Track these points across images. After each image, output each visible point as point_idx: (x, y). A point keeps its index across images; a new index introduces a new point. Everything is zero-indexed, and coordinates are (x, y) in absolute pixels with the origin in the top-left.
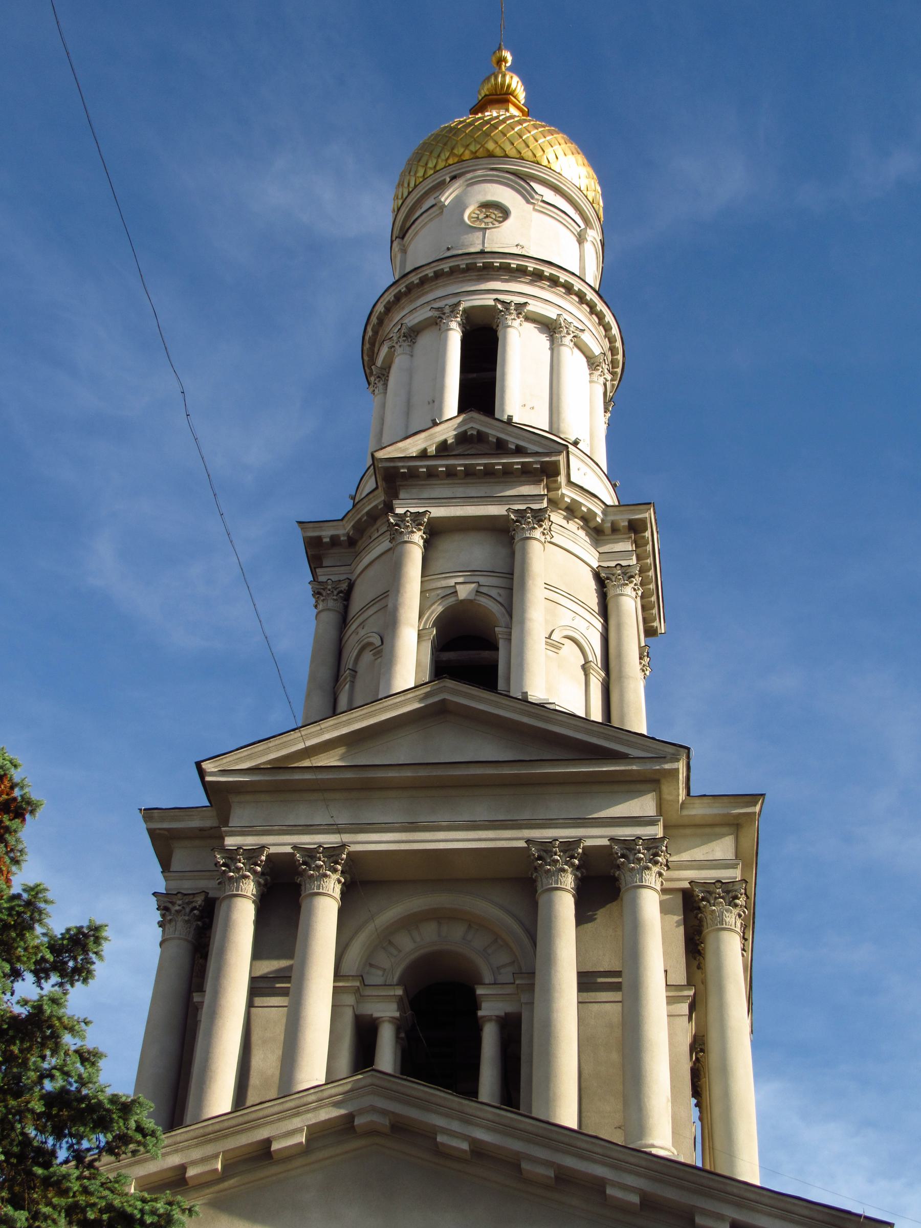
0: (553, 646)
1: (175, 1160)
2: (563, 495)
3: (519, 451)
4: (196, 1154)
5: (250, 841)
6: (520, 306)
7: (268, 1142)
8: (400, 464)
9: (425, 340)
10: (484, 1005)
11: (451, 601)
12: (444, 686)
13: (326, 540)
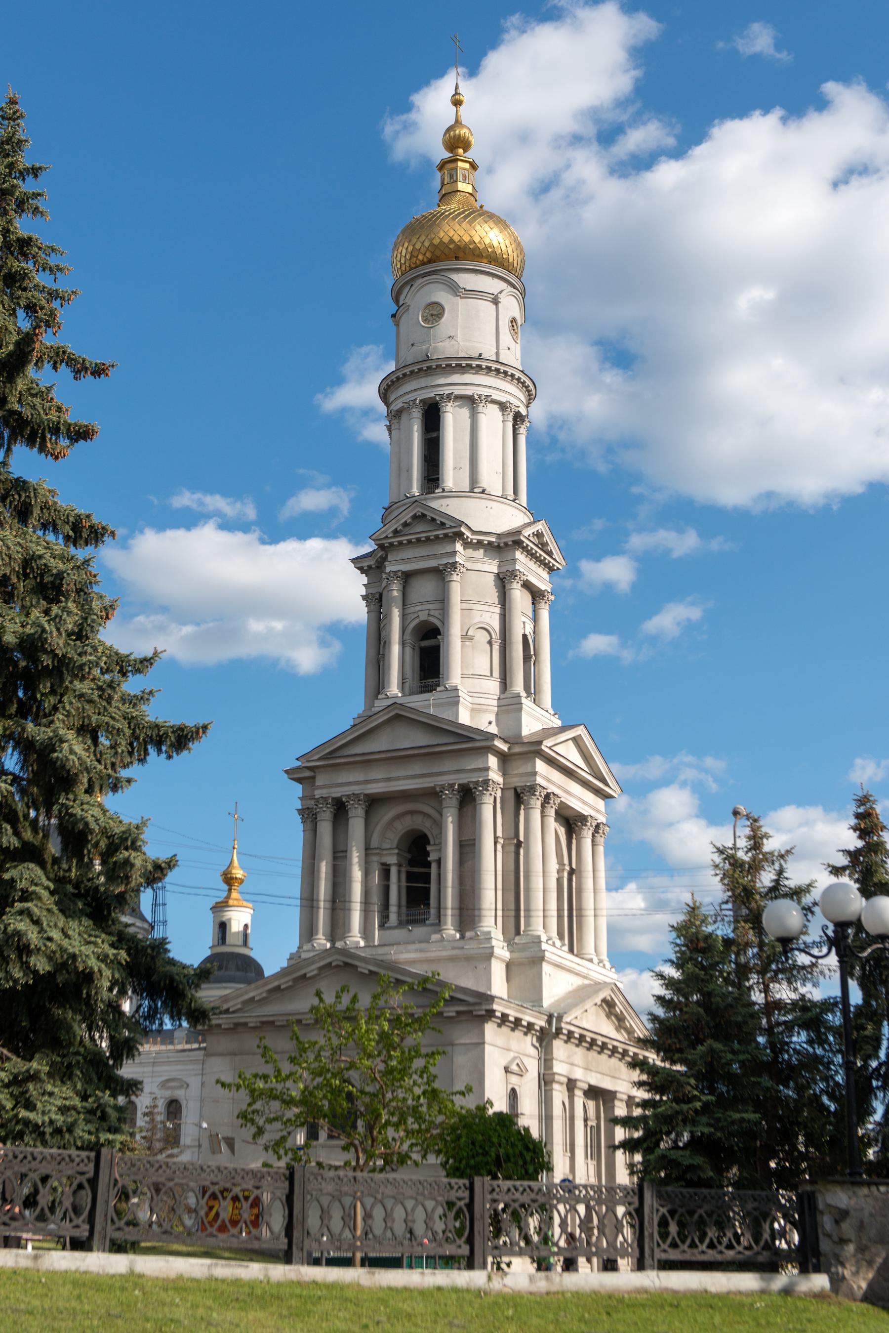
1: (276, 984)
3: (443, 524)
4: (283, 981)
5: (324, 792)
6: (449, 396)
7: (305, 975)
9: (404, 417)
10: (431, 855)
11: (416, 621)
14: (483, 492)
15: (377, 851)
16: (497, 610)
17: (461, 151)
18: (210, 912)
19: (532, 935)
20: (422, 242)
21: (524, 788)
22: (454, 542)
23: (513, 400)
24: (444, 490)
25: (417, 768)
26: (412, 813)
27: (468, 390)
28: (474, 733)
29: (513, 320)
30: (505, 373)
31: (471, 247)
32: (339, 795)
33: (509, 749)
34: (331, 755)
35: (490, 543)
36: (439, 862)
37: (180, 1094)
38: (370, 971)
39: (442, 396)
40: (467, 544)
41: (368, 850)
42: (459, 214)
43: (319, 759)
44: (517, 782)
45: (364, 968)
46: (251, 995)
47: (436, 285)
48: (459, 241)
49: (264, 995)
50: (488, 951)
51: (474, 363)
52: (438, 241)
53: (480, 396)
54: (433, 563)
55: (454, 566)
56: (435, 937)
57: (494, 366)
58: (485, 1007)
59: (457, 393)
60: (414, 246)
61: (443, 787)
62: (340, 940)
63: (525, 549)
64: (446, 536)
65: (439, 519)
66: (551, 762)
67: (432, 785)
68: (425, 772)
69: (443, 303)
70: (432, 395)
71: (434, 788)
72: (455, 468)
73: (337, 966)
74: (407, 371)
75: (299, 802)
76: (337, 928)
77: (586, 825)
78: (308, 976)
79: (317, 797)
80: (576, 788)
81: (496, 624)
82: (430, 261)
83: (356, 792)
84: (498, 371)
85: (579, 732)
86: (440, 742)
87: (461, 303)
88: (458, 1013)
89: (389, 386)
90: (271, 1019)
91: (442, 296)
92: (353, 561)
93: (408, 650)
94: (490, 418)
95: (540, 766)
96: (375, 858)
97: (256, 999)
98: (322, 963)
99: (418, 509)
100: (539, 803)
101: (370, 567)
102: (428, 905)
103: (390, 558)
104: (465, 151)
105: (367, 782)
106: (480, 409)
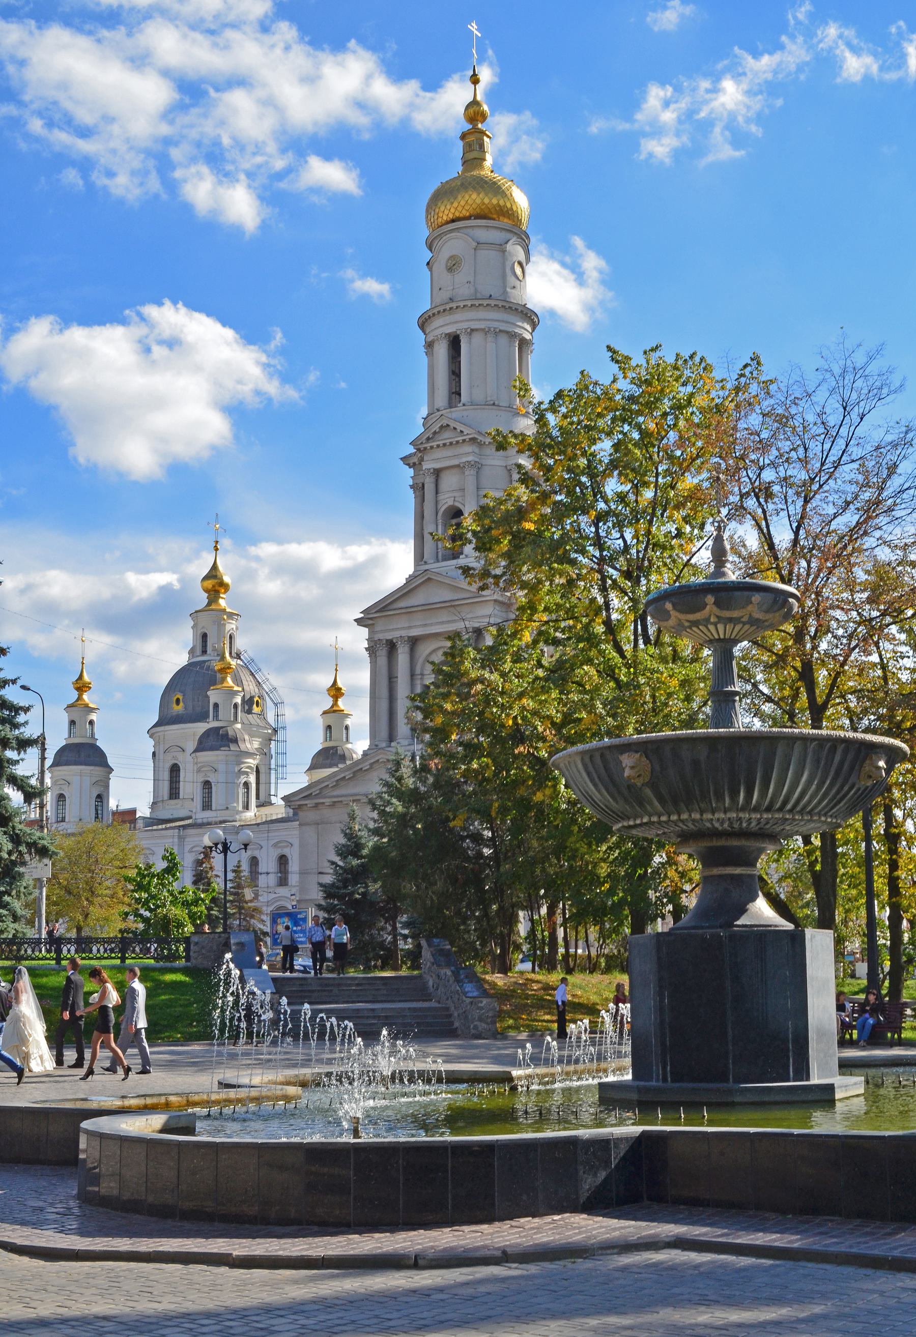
1: (343, 775)
3: (462, 432)
4: (347, 773)
25: (444, 616)
37: (286, 851)
41: (412, 675)
43: (376, 612)
54: (455, 462)
64: (464, 441)
68: (450, 619)
74: (435, 311)
82: (453, 221)
90: (340, 799)
98: (372, 761)
101: (414, 464)
103: (425, 458)
105: (410, 627)
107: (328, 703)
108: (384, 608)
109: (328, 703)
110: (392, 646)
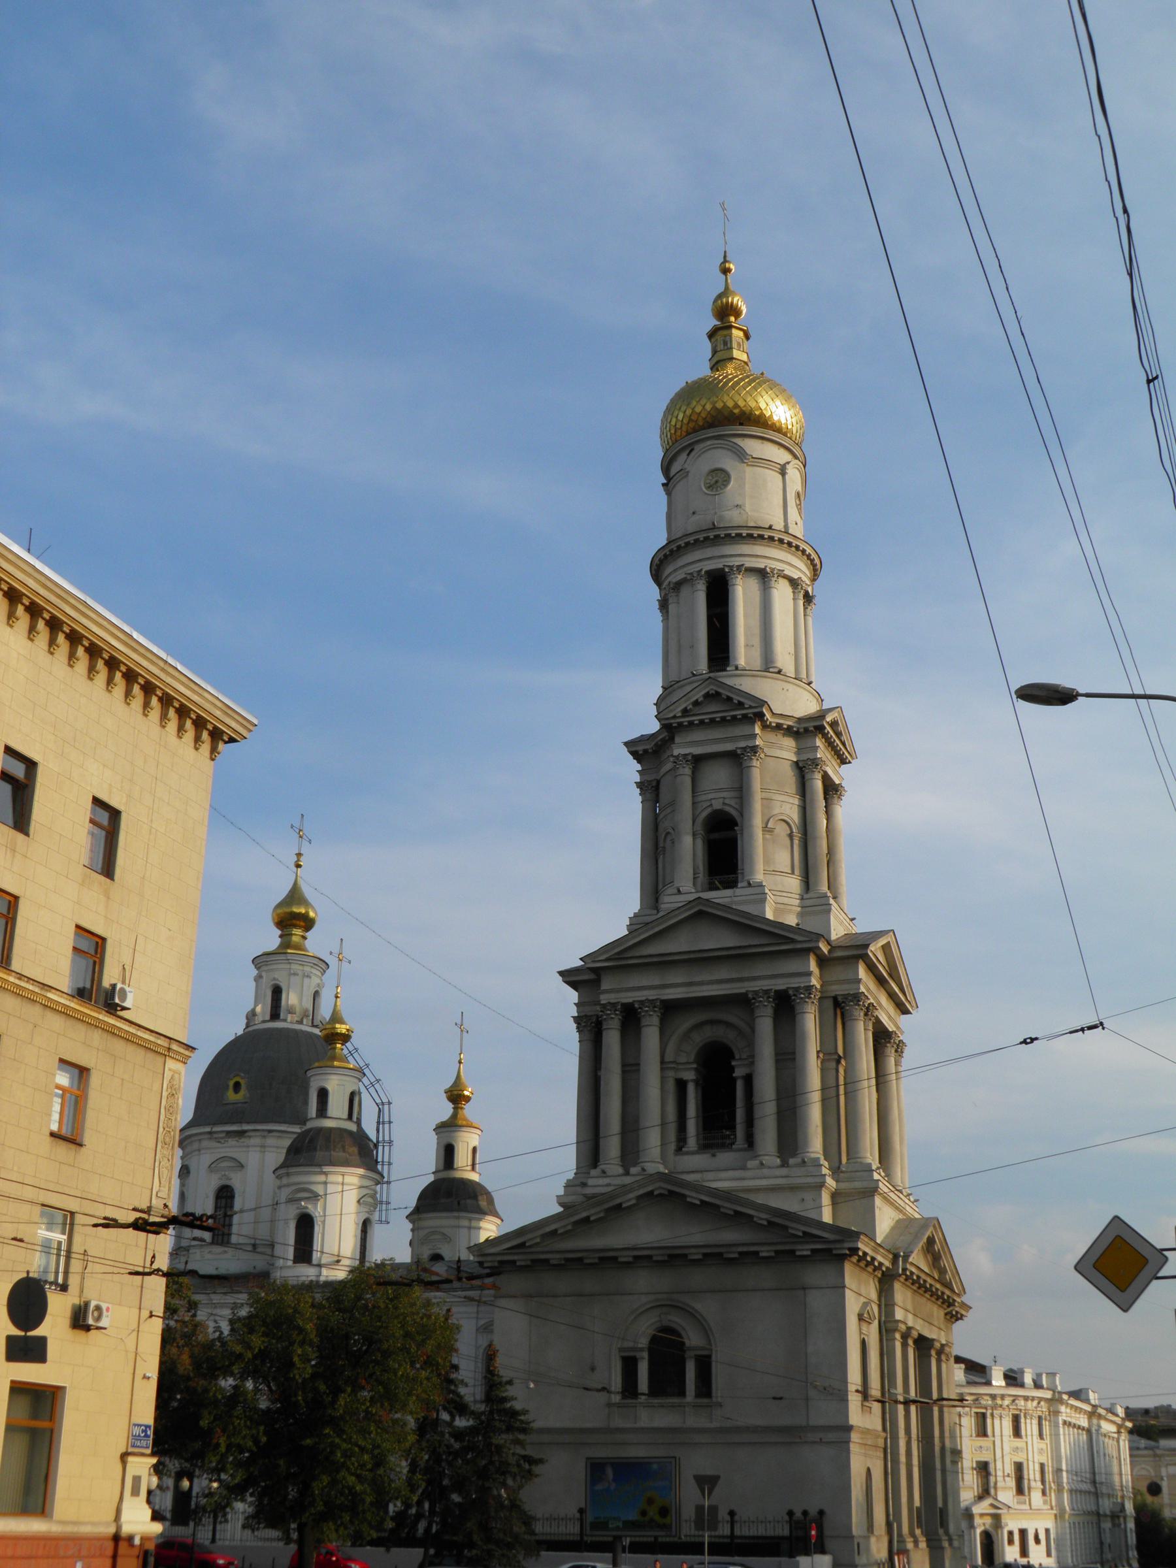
0: (769, 831)
1: (584, 1214)
2: (770, 723)
3: (741, 705)
4: (593, 1211)
6: (739, 567)
7: (620, 1204)
8: (672, 721)
9: (685, 591)
10: (736, 1070)
11: (709, 810)
12: (699, 898)
13: (641, 752)
14: (779, 672)
15: (673, 1066)
16: (796, 801)
17: (732, 319)
18: (434, 1133)
19: (861, 1163)
20: (702, 407)
21: (846, 996)
22: (753, 723)
23: (804, 578)
24: (737, 668)
25: (723, 972)
26: (712, 1022)
27: (760, 564)
28: (795, 933)
29: (798, 495)
30: (797, 547)
31: (757, 413)
32: (630, 1000)
33: (830, 952)
34: (619, 956)
35: (789, 728)
36: (749, 1080)
38: (702, 1201)
39: (731, 567)
40: (766, 726)
42: (742, 379)
44: (838, 990)
45: (694, 1197)
46: (553, 1227)
47: (719, 450)
48: (745, 406)
49: (570, 1227)
50: (818, 1180)
51: (767, 534)
52: (722, 405)
53: (773, 570)
54: (729, 747)
55: (754, 749)
56: (751, 1164)
57: (787, 539)
58: (847, 1245)
59: (748, 565)
60: (693, 409)
61: (756, 992)
62: (635, 1164)
63: (825, 736)
64: (745, 716)
65: (736, 698)
66: (872, 968)
67: (743, 991)
68: (734, 975)
69: (728, 468)
70: (720, 566)
71: (746, 994)
72: (747, 646)
73: (661, 1195)
74: (691, 539)
75: (575, 1008)
76: (630, 1153)
77: (890, 1042)
78: (624, 1205)
79: (602, 1002)
80: (883, 999)
81: (794, 815)
83: (651, 998)
84: (790, 544)
85: (889, 939)
86: (752, 943)
87: (749, 471)
88: (813, 1251)
89: (666, 556)
91: (728, 463)
92: (626, 744)
93: (699, 842)
94: (782, 594)
95: (862, 972)
96: (671, 1074)
97: (559, 1232)
98: (641, 1192)
99: (712, 687)
100: (862, 1014)
101: (646, 751)
102: (732, 1127)
103: (677, 740)
104: (736, 320)
106: (773, 583)
107: (445, 1110)
108: (618, 953)
109: (445, 1110)
110: (631, 1016)
